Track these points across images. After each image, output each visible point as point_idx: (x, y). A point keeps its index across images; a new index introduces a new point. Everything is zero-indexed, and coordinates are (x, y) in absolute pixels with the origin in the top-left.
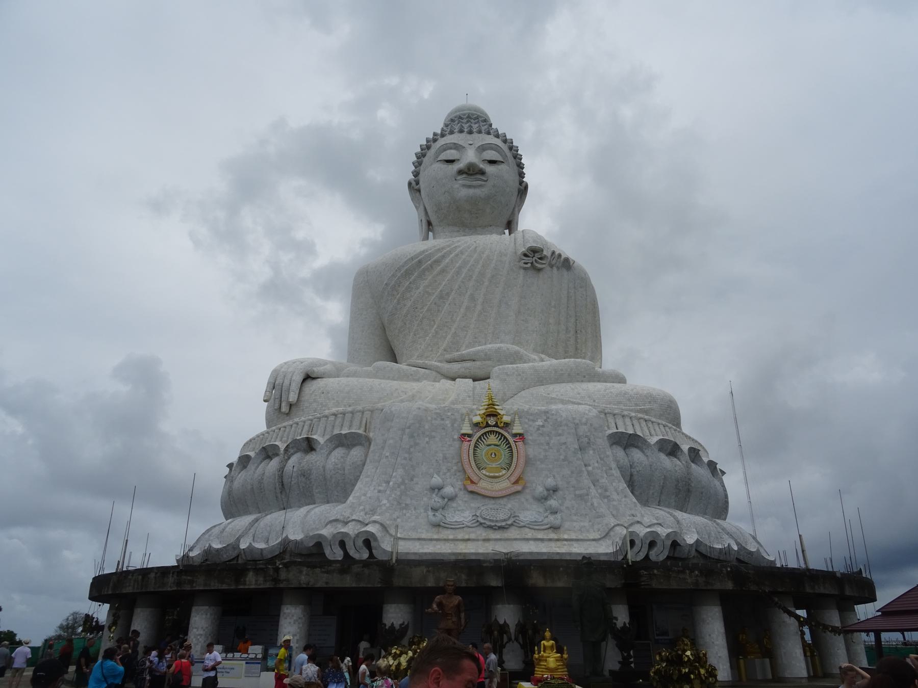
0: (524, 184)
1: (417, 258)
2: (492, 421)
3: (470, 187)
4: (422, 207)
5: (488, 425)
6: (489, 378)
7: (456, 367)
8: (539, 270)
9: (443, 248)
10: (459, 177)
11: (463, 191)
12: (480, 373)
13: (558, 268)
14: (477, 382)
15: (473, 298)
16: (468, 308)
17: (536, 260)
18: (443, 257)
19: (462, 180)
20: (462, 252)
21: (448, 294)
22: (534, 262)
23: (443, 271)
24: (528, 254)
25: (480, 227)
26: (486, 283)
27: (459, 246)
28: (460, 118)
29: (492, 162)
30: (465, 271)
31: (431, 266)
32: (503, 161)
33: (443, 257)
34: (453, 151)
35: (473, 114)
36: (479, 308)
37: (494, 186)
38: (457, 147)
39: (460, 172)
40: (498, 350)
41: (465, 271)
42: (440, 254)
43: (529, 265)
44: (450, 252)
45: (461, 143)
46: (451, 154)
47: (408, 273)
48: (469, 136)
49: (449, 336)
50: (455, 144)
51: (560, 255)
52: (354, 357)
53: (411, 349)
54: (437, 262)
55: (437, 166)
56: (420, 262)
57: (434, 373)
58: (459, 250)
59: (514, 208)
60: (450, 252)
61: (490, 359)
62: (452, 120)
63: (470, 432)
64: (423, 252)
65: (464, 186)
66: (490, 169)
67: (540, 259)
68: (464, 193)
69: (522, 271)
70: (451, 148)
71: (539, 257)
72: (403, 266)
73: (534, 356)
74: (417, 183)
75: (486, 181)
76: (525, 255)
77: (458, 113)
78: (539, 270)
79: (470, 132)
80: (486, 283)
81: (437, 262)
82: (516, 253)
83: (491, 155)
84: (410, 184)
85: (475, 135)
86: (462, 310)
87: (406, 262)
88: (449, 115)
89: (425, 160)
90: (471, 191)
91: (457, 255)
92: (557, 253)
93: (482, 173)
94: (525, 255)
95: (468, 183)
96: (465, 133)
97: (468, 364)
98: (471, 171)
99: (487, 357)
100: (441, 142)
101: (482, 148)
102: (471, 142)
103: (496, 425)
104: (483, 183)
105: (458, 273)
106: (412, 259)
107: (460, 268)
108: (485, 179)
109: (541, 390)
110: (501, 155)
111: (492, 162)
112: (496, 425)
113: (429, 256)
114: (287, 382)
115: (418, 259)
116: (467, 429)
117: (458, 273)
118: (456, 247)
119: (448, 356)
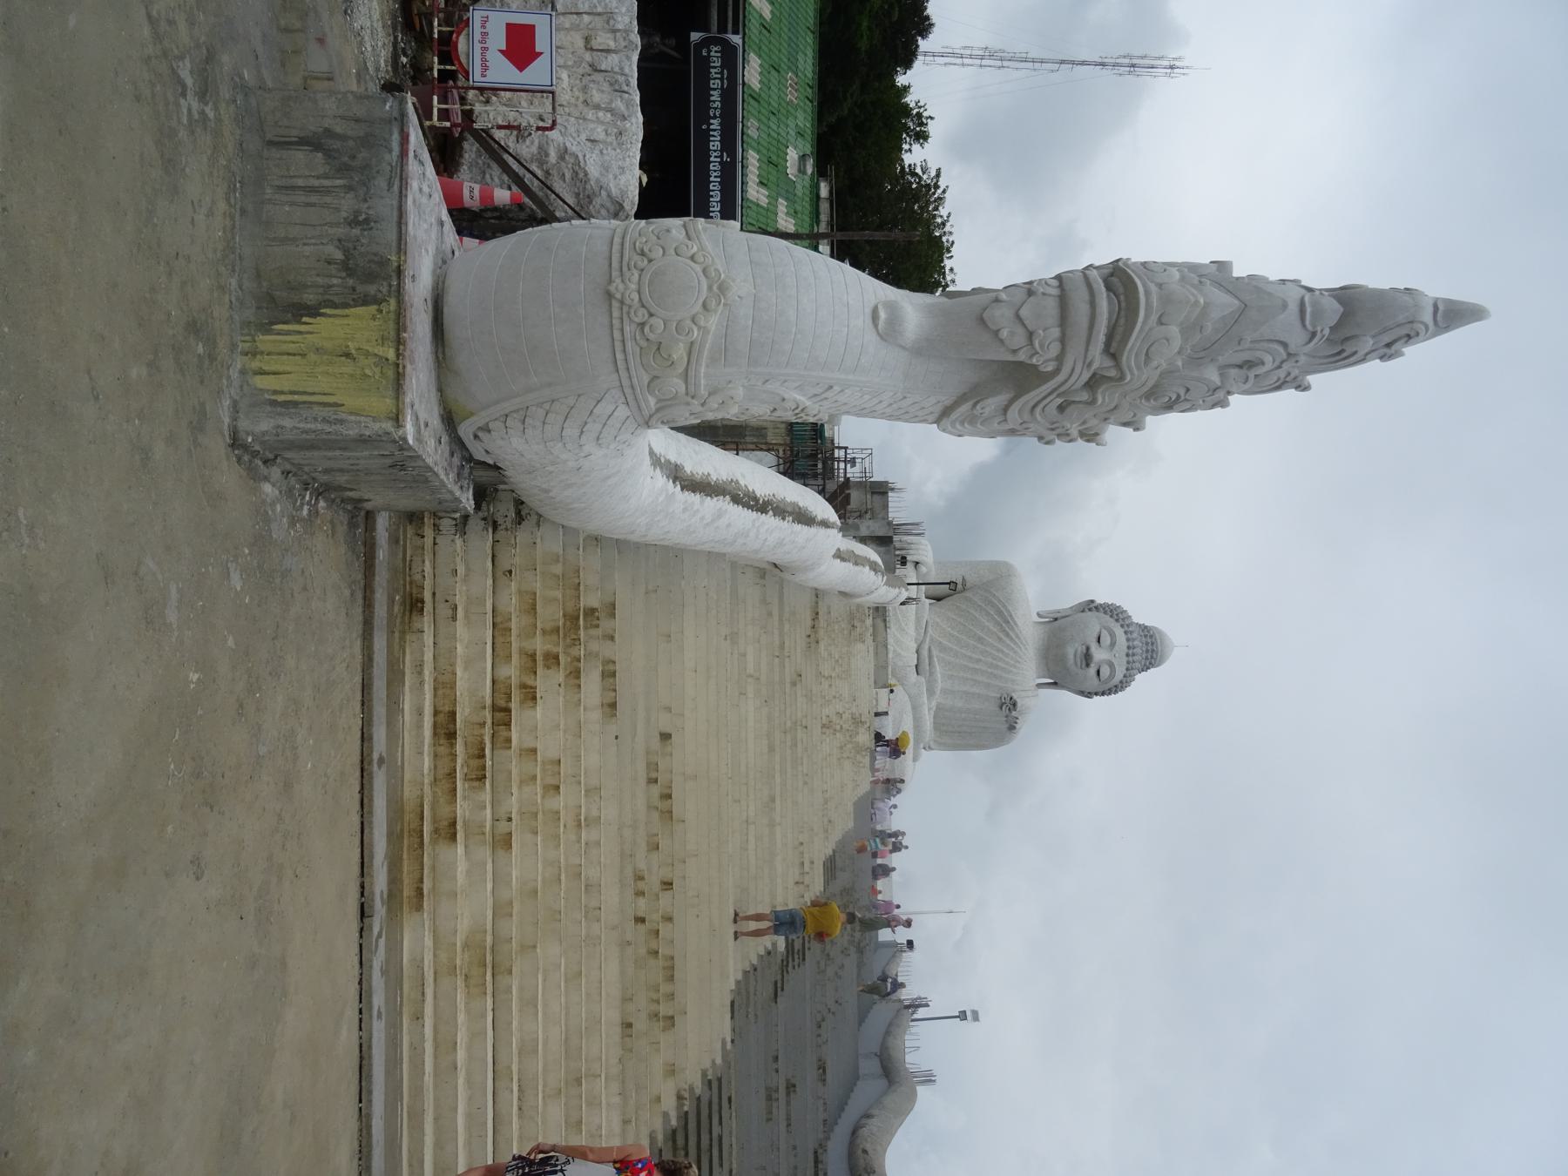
3: (1075, 656)
6: (918, 674)
7: (925, 653)
9: (1019, 638)
10: (1084, 647)
11: (1072, 651)
12: (920, 668)
13: (1006, 721)
14: (914, 668)
15: (978, 661)
16: (970, 658)
18: (1012, 639)
19: (1081, 649)
20: (1015, 652)
21: (982, 644)
23: (1000, 639)
26: (989, 670)
27: (1021, 650)
29: (1098, 673)
30: (1000, 655)
31: (1004, 631)
33: (1012, 639)
34: (1109, 642)
35: (1157, 654)
36: (971, 665)
37: (1077, 674)
38: (1113, 644)
39: (1088, 649)
40: (936, 681)
41: (1000, 655)
42: (1014, 637)
44: (1015, 643)
45: (1116, 648)
46: (1106, 639)
47: (1000, 613)
48: (1125, 654)
49: (950, 645)
51: (1016, 723)
54: (1008, 635)
55: (1097, 628)
57: (921, 639)
58: (1019, 651)
60: (1015, 643)
64: (1016, 624)
65: (1076, 652)
66: (1092, 671)
67: (1009, 709)
68: (1070, 652)
69: (999, 696)
70: (1111, 640)
72: (1006, 609)
73: (934, 704)
74: (1090, 610)
75: (1081, 668)
76: (1011, 698)
77: (1159, 641)
78: (1001, 708)
79: (1127, 655)
80: (989, 670)
81: (1008, 635)
82: (1014, 691)
83: (1105, 671)
84: (1092, 601)
85: (1125, 659)
86: (969, 654)
87: (1009, 611)
88: (1160, 632)
89: (1107, 617)
90: (1071, 656)
91: (1013, 649)
92: (1018, 721)
93: (1088, 665)
94: (1011, 698)
95: (1078, 656)
98: (1087, 657)
99: (931, 673)
100: (1119, 632)
101: (1111, 665)
102: (1117, 655)
105: (999, 650)
107: (1003, 652)
109: (909, 708)
111: (1098, 673)
114: (911, 552)
117: (999, 650)
119: (932, 648)
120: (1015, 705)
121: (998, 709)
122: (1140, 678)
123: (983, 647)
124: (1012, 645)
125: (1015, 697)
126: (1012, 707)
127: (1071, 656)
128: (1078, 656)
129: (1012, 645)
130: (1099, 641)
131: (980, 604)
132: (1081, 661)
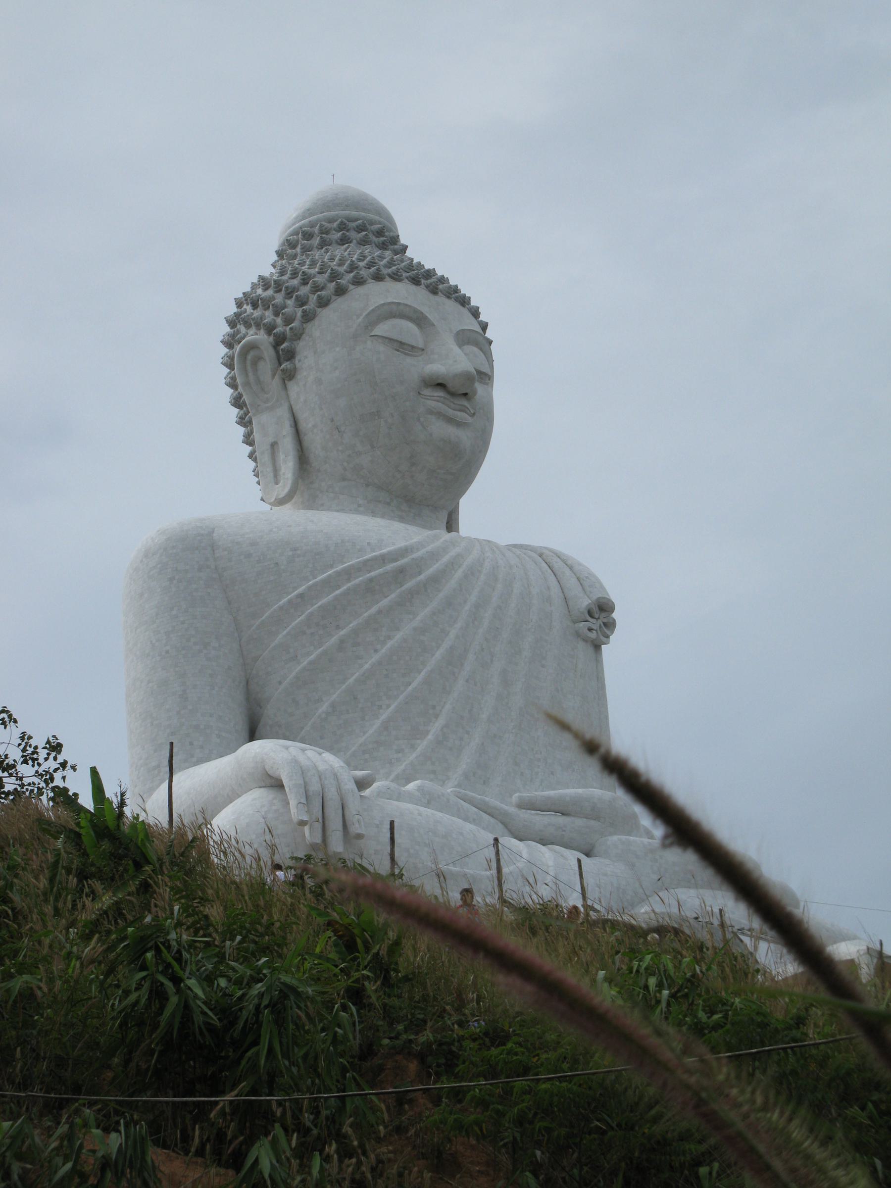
1: (396, 560)
4: (283, 412)
10: (427, 392)
25: (428, 506)
44: (453, 565)
46: (408, 331)
47: (371, 589)
52: (191, 744)
53: (367, 756)
61: (597, 818)
65: (440, 415)
71: (605, 620)
96: (423, 286)
97: (561, 820)
106: (383, 559)
113: (418, 566)
115: (399, 563)
123: (471, 657)
124: (459, 574)
126: (603, 618)
129: (459, 574)
131: (334, 640)
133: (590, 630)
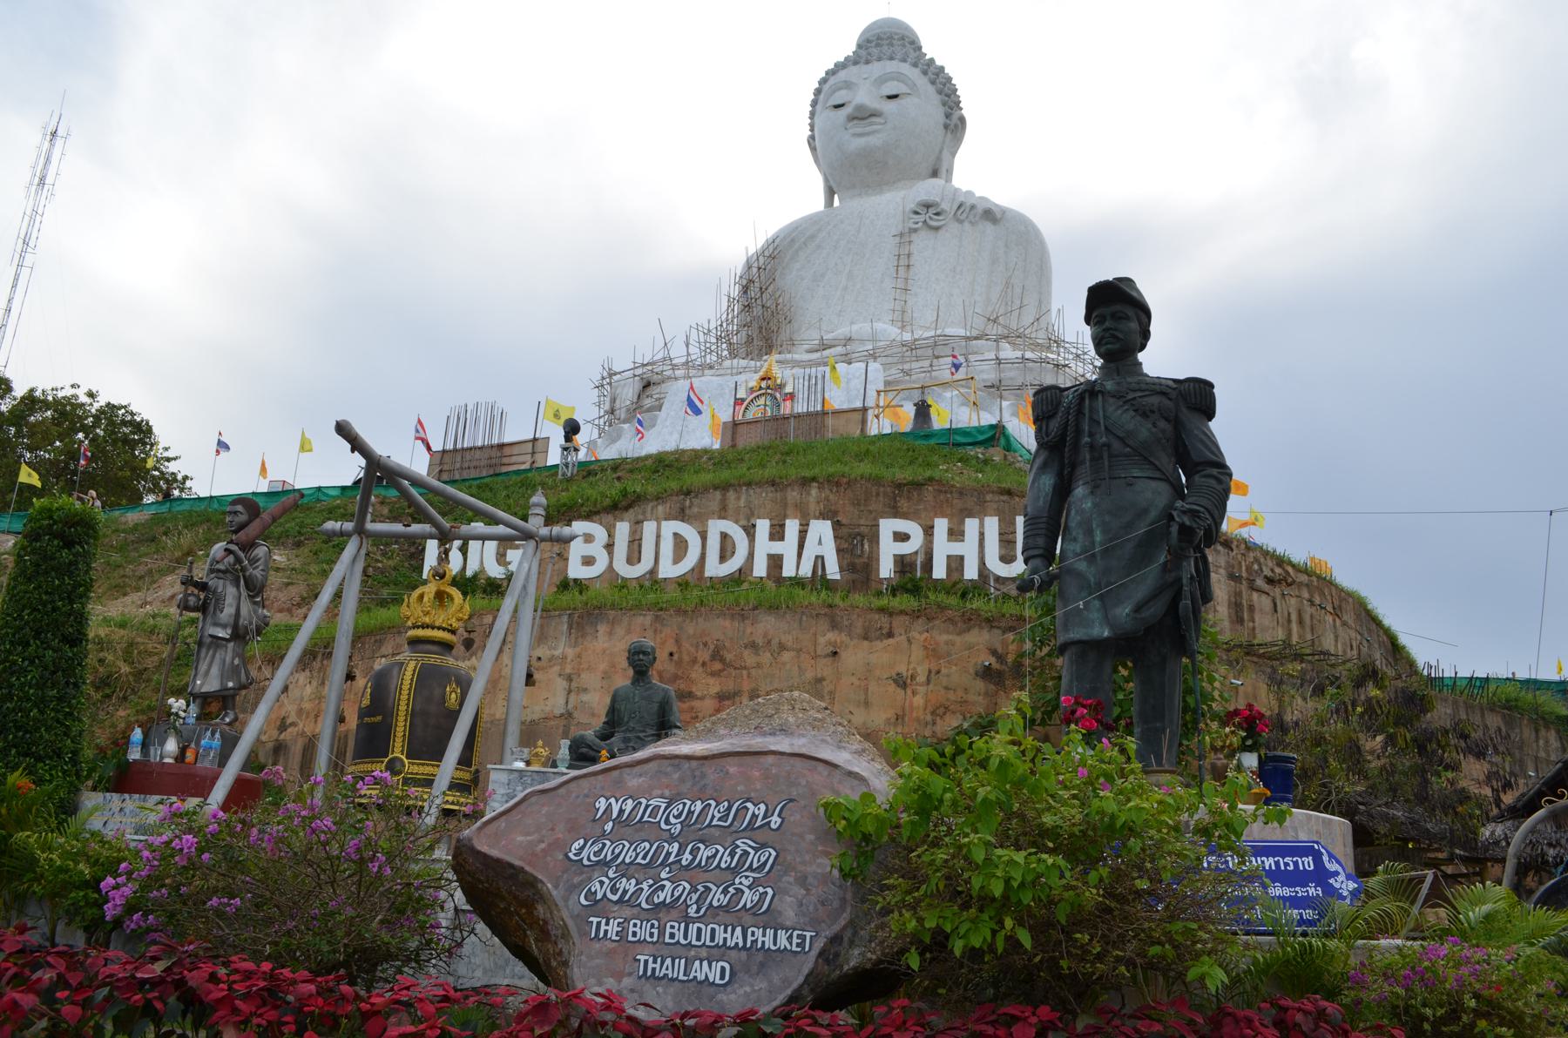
0: (955, 118)
2: (764, 384)
5: (761, 388)
8: (937, 229)
17: (930, 218)
18: (819, 230)
21: (823, 275)
22: (928, 220)
24: (918, 210)
28: (879, 38)
31: (805, 243)
32: (909, 91)
33: (819, 230)
34: (843, 92)
38: (848, 85)
43: (920, 224)
50: (845, 82)
54: (812, 237)
56: (793, 240)
59: (941, 152)
62: (869, 41)
63: (744, 396)
67: (937, 214)
70: (840, 89)
76: (916, 213)
78: (937, 229)
81: (812, 237)
90: (861, 141)
95: (859, 130)
101: (881, 81)
102: (865, 76)
103: (768, 388)
104: (879, 127)
108: (883, 121)
110: (906, 84)
112: (768, 388)
116: (741, 394)
118: (836, 215)
120: (928, 206)
121: (941, 232)
122: (929, 50)
125: (912, 206)
126: (932, 211)
127: (861, 141)
128: (859, 130)
130: (842, 105)
132: (871, 124)
133: (917, 223)
